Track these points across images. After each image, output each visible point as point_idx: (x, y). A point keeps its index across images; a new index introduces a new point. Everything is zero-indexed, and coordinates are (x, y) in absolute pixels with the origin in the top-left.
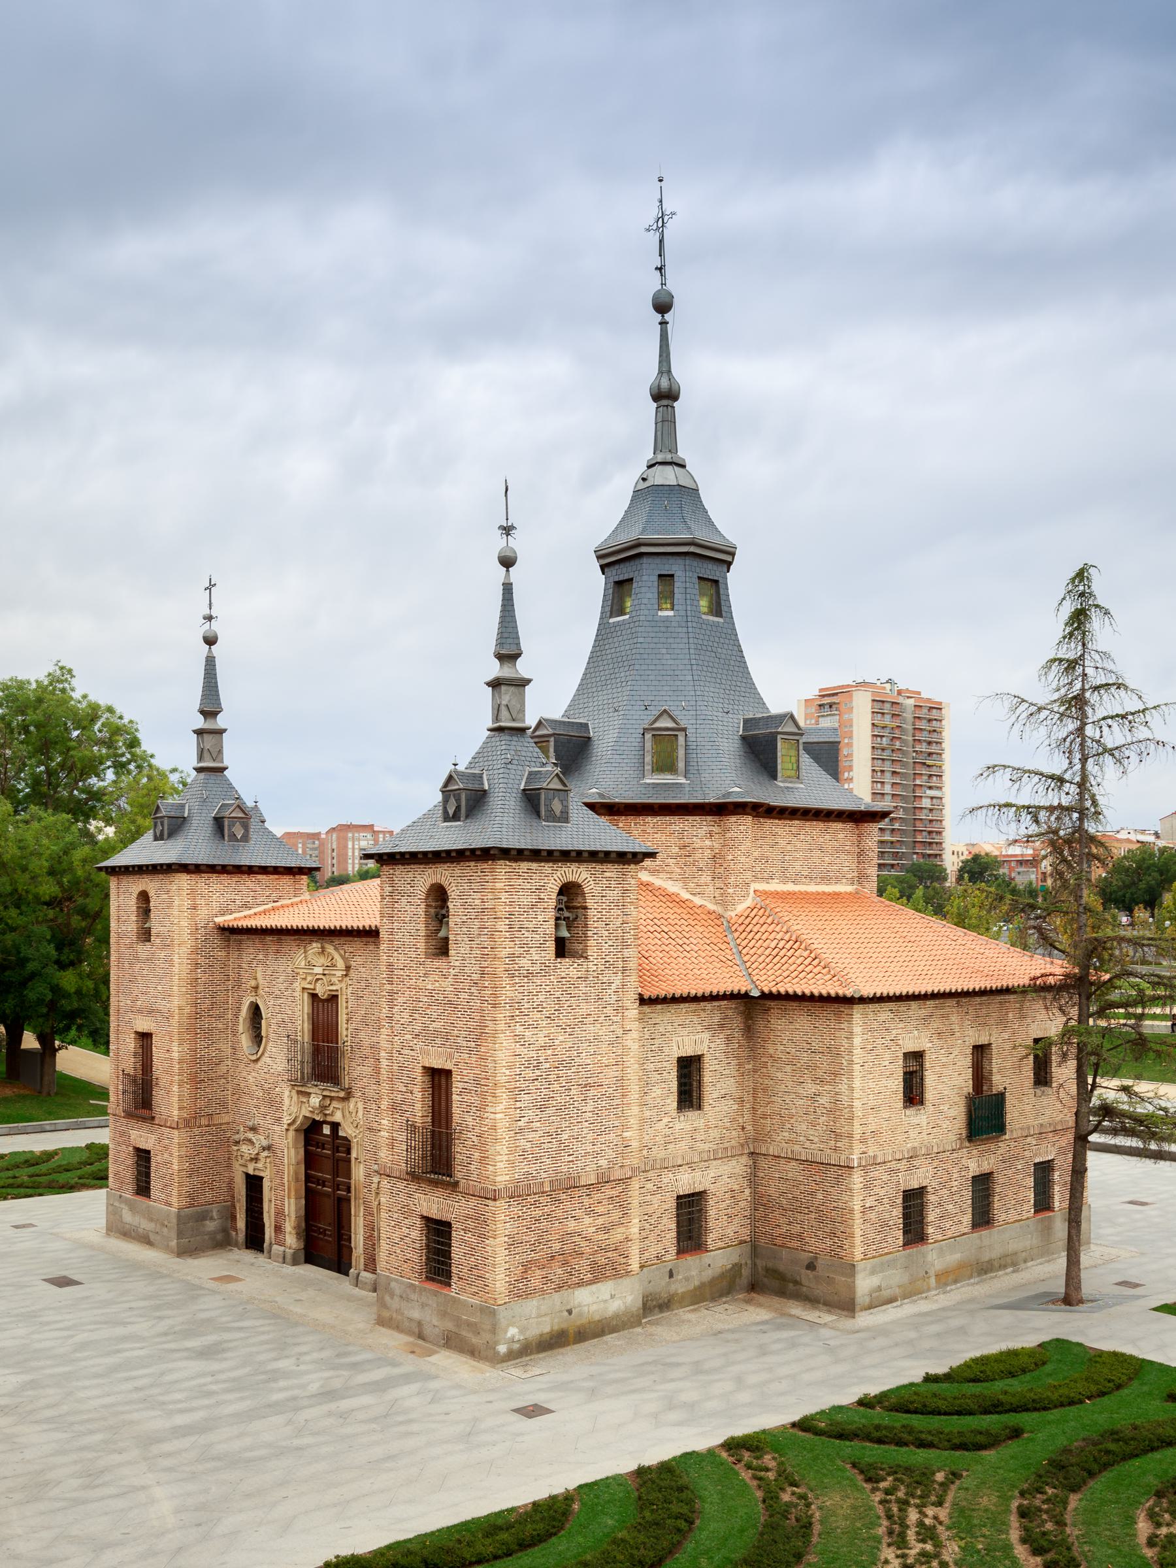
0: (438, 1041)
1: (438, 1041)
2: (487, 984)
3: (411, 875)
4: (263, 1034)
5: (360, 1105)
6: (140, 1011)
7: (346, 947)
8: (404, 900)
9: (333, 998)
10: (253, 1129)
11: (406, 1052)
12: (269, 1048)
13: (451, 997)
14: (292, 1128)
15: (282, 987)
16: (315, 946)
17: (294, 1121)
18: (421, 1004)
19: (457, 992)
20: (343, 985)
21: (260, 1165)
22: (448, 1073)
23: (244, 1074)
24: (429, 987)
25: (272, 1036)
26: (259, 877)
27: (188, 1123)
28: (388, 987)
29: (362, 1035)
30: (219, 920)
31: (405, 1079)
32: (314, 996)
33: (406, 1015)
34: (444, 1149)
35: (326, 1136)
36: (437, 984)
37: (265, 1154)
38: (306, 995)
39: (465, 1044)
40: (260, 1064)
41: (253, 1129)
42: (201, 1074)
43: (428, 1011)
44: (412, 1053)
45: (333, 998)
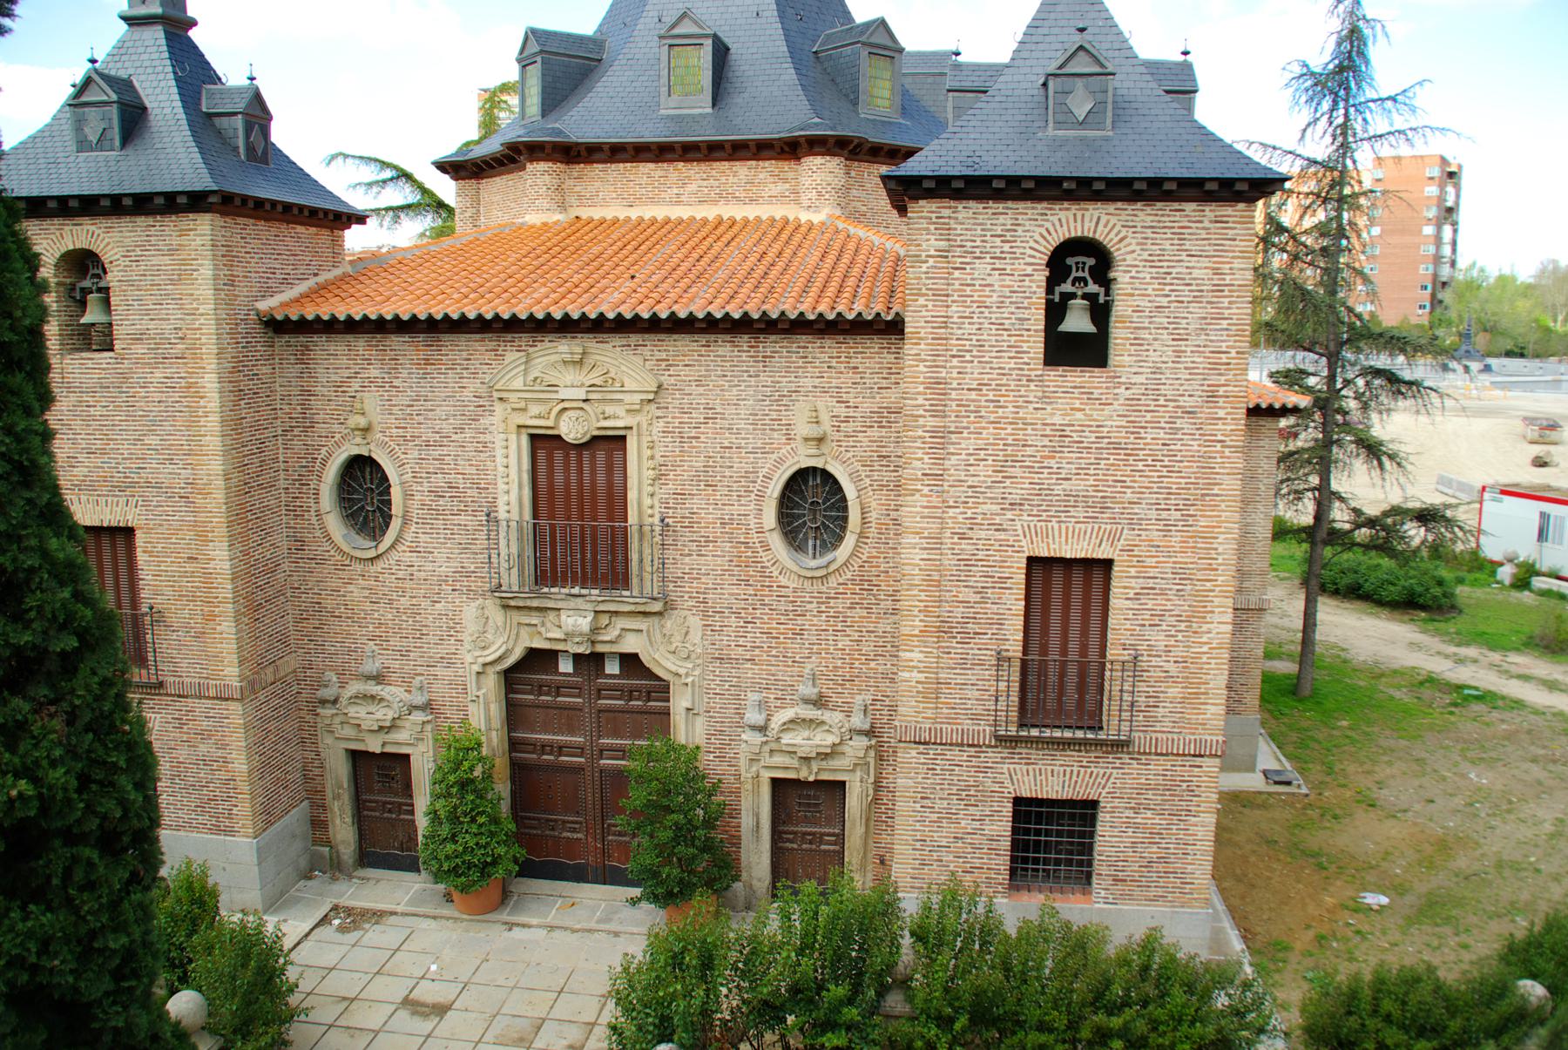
0: (1080, 513)
1: (1080, 513)
2: (1221, 413)
3: (1006, 220)
4: (397, 509)
5: (695, 622)
7: (646, 351)
8: (982, 268)
9: (613, 443)
10: (379, 678)
11: (983, 534)
12: (409, 536)
13: (1120, 436)
14: (491, 670)
15: (447, 428)
16: (566, 347)
17: (500, 659)
18: (1029, 451)
19: (1136, 429)
20: (642, 419)
21: (402, 736)
22: (1108, 564)
23: (335, 583)
24: (1057, 420)
25: (415, 513)
26: (300, 229)
27: (251, 687)
28: (931, 422)
29: (695, 503)
30: (263, 306)
31: (977, 580)
32: (543, 443)
33: (984, 472)
34: (1092, 689)
35: (565, 674)
36: (1079, 415)
37: (419, 717)
38: (525, 441)
39: (1153, 514)
40: (379, 566)
41: (379, 678)
42: (277, 602)
43: (1052, 463)
44: (1002, 536)
45: (613, 443)
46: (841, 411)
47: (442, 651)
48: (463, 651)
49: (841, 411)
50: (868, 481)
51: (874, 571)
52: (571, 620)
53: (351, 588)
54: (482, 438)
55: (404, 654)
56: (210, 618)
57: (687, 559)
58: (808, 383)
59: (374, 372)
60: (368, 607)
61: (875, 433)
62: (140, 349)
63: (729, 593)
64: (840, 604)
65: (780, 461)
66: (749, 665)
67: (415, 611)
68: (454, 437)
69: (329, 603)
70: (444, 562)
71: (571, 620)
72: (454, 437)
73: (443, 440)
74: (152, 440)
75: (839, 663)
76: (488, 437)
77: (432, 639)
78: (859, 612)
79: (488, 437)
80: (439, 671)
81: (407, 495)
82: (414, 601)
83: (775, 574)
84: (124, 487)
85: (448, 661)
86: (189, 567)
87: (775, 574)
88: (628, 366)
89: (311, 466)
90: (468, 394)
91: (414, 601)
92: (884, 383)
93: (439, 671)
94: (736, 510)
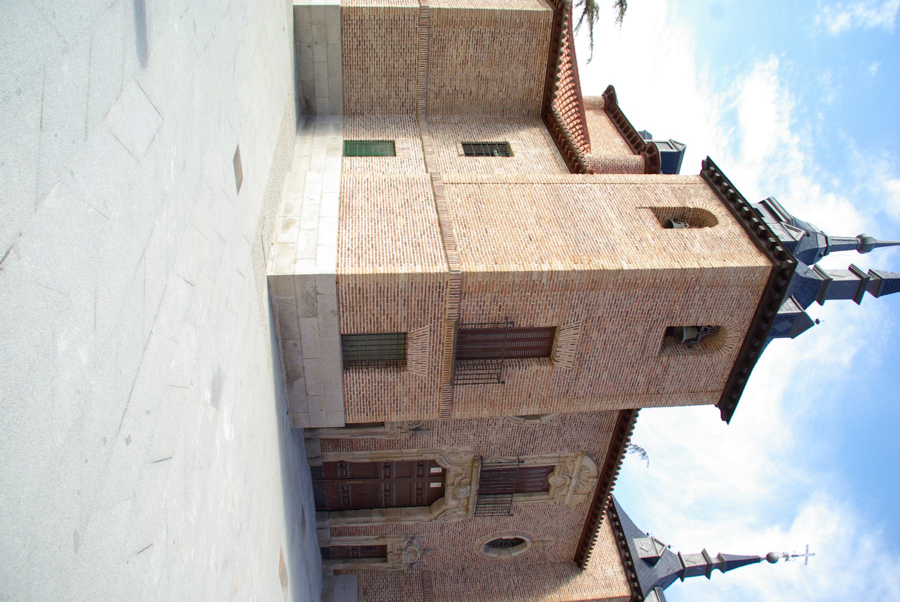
6: (586, 335)
56: (492, 404)
58: (561, 540)
62: (659, 370)
74: (605, 375)
76: (558, 451)
77: (453, 434)
80: (435, 437)
84: (581, 359)
85: (441, 440)
86: (525, 394)
90: (581, 443)
93: (435, 437)
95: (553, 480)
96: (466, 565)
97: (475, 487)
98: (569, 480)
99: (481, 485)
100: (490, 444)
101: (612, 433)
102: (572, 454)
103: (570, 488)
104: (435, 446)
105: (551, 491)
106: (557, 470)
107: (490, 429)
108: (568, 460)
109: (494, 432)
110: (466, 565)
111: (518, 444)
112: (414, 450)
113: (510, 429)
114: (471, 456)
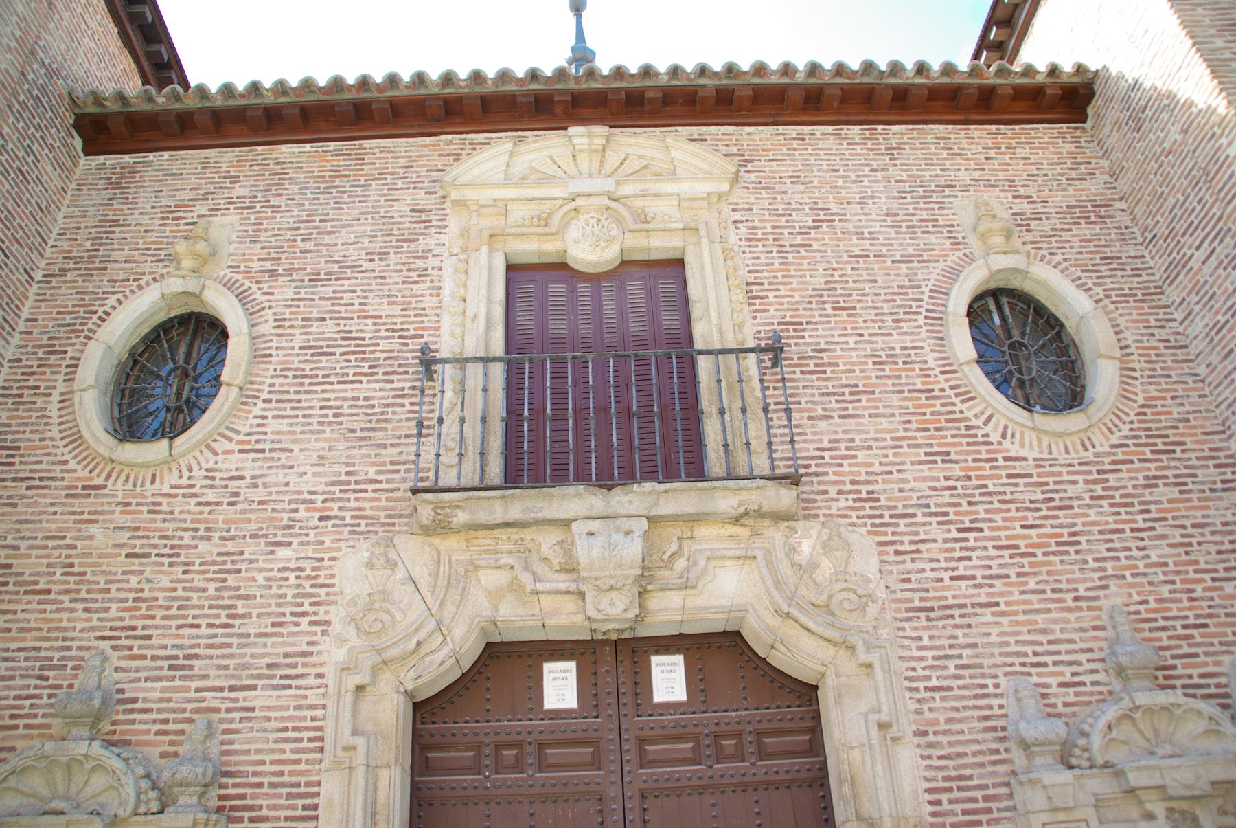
46: (1026, 207)
47: (274, 649)
48: (326, 644)
49: (1026, 207)
50: (1099, 290)
51: (1165, 421)
52: (589, 558)
53: (93, 530)
54: (420, 264)
55: (178, 666)
57: (823, 425)
58: (964, 176)
59: (238, 191)
60: (120, 564)
61: (1085, 230)
63: (916, 480)
64: (1126, 480)
65: (953, 274)
66: (987, 616)
67: (228, 564)
68: (366, 266)
69: (30, 565)
70: (310, 463)
71: (589, 558)
72: (366, 266)
73: (346, 267)
75: (1165, 591)
78: (1165, 493)
79: (432, 262)
80: (259, 698)
81: (259, 356)
82: (230, 546)
83: (995, 437)
85: (283, 673)
87: (995, 437)
88: (679, 171)
89: (84, 320)
90: (403, 207)
91: (230, 546)
92: (1073, 174)
93: (259, 698)
94: (896, 341)
95: (589, 250)
96: (1208, 474)
97: (573, 501)
98: (580, 202)
99: (560, 478)
100: (352, 484)
101: (367, 143)
102: (454, 224)
103: (628, 189)
104: (313, 697)
105: (659, 245)
106: (530, 249)
107: (260, 494)
108: (489, 222)
109: (280, 476)
110: (1208, 474)
111: (365, 388)
112: (330, 788)
113: (273, 425)
114: (414, 553)
